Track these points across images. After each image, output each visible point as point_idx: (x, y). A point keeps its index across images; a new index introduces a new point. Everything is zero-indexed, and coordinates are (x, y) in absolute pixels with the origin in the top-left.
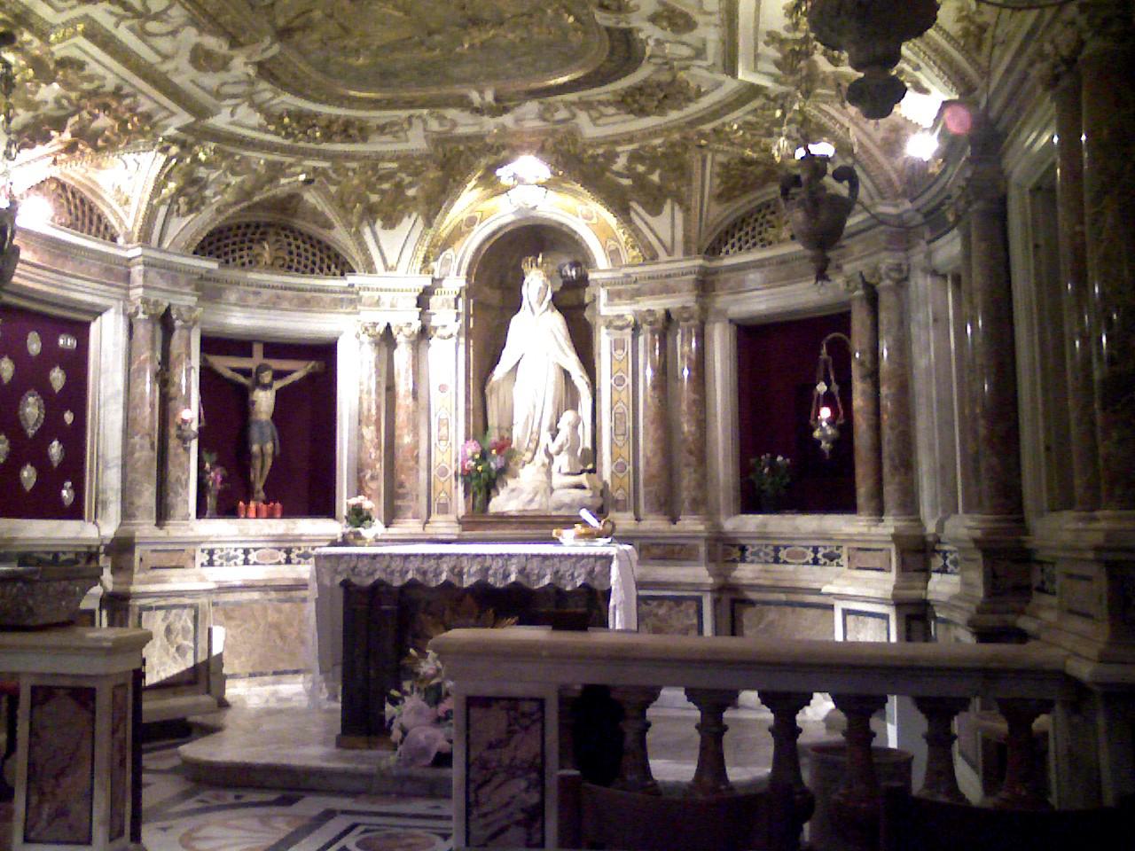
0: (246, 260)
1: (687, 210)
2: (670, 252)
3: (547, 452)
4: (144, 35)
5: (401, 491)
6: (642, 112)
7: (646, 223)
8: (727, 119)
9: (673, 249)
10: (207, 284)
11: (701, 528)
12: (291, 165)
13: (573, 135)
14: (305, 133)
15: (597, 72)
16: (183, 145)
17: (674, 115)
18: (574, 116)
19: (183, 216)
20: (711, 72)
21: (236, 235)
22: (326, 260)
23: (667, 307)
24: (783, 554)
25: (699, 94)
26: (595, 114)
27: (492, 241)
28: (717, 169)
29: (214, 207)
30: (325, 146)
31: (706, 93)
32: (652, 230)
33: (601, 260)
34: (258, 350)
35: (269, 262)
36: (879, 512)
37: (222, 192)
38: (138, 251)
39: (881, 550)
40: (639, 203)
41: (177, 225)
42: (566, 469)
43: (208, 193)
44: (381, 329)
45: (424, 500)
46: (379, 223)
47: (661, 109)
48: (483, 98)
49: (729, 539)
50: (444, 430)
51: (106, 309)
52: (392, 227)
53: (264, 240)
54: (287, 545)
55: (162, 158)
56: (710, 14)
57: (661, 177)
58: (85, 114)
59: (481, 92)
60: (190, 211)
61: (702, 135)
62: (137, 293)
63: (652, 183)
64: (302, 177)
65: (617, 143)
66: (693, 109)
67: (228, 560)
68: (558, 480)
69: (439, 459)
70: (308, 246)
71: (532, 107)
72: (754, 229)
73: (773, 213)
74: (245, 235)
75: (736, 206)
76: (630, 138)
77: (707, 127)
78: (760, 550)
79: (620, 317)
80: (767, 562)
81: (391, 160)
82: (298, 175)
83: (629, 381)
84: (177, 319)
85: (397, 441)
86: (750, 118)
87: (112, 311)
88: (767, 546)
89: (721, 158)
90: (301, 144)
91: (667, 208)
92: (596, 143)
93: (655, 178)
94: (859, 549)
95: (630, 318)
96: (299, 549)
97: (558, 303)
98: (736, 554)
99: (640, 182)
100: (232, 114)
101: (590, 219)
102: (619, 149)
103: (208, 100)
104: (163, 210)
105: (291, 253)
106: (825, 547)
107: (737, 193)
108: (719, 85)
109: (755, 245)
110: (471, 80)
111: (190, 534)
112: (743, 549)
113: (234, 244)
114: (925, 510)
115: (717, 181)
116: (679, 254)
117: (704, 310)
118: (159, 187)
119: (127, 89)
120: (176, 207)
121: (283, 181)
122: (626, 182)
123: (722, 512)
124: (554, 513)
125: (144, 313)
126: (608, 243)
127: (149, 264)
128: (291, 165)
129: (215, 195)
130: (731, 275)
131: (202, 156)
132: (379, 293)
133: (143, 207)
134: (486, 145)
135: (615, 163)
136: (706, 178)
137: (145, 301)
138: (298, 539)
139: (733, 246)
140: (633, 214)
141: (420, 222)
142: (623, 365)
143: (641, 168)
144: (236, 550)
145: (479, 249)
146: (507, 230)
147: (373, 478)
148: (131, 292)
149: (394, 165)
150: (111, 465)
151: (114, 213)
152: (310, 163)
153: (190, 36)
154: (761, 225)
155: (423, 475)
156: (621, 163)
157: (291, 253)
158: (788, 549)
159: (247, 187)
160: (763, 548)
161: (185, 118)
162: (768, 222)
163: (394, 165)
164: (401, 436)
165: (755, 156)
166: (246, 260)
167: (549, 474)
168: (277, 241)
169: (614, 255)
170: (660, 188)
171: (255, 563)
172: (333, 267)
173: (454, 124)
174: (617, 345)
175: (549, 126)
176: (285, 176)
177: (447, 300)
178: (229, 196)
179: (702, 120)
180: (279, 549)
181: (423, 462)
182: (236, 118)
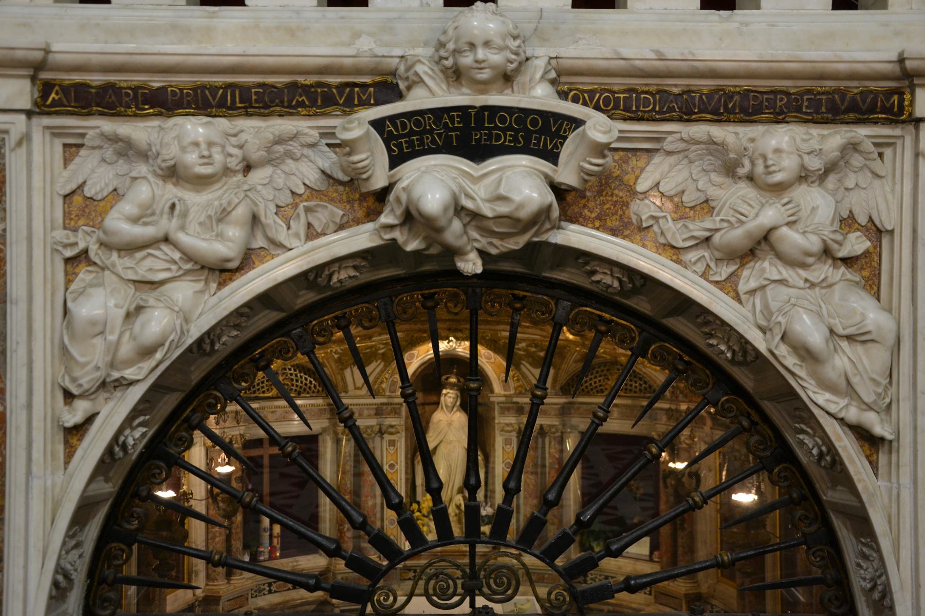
7: (530, 371)
27: (422, 367)
67: (260, 592)
73: (608, 370)
79: (507, 425)
87: (198, 445)
97: (464, 407)
101: (490, 359)
117: (564, 425)
122: (522, 353)
140: (522, 366)
141: (383, 364)
143: (533, 349)
144: (264, 585)
157: (292, 380)
168: (284, 373)
171: (275, 592)
177: (394, 408)
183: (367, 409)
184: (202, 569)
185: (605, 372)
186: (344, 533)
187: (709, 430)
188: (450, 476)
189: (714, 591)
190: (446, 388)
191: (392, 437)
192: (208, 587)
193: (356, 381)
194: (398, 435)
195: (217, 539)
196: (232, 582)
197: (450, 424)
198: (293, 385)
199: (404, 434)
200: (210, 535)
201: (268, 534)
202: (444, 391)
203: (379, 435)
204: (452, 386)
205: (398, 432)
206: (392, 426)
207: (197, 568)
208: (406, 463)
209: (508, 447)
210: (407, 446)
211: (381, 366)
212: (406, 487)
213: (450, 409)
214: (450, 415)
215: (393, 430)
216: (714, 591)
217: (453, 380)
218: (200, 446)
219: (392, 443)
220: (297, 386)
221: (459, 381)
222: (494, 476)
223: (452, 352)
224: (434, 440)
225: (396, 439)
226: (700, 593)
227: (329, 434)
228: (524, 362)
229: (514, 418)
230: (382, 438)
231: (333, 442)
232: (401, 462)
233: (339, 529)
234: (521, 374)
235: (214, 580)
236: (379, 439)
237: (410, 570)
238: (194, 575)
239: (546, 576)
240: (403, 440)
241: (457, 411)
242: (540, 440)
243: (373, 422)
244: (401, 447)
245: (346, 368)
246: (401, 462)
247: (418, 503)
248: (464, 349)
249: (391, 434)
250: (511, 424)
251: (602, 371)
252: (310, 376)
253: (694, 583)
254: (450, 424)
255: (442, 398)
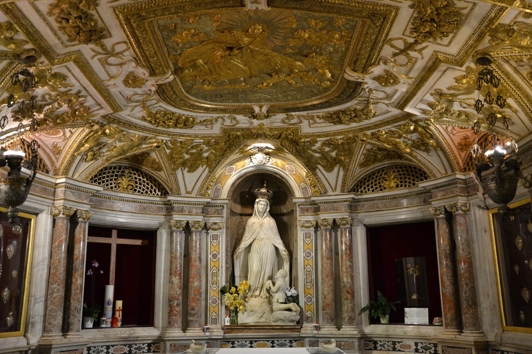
0: (113, 185)
1: (346, 171)
2: (334, 190)
3: (268, 291)
4: (104, 63)
5: (193, 312)
6: (340, 122)
7: (324, 175)
8: (381, 129)
9: (335, 190)
10: (95, 198)
11: (356, 332)
12: (151, 138)
13: (296, 131)
14: (164, 122)
15: (326, 102)
16: (102, 126)
17: (354, 125)
18: (301, 122)
19: (88, 162)
20: (388, 107)
21: (109, 173)
22: (154, 187)
23: (334, 218)
24: (398, 346)
25: (374, 115)
26: (311, 121)
27: (240, 180)
28: (365, 152)
29: (104, 158)
30: (171, 130)
31: (378, 115)
32: (326, 179)
33: (298, 193)
34: (114, 233)
35: (125, 187)
36: (460, 327)
37: (112, 150)
38: (63, 180)
39: (465, 348)
40: (321, 165)
41: (84, 166)
42: (282, 300)
43: (104, 150)
44: (184, 224)
45: (203, 316)
46: (187, 169)
47: (352, 120)
48: (261, 111)
49: (368, 337)
50: (215, 278)
51: (42, 211)
52: (194, 171)
53: (123, 175)
54: (130, 343)
55: (87, 131)
56: (411, 78)
57: (337, 154)
58: (56, 105)
59: (261, 107)
60: (92, 160)
61: (365, 135)
62: (59, 203)
63: (331, 157)
64: (155, 144)
65: (319, 136)
66: (365, 123)
68: (276, 306)
69: (212, 294)
70: (145, 179)
71: (282, 116)
72: (376, 181)
73: (386, 174)
74: (113, 172)
75: (369, 168)
76: (327, 135)
77: (369, 133)
78: (385, 344)
80: (389, 350)
81: (201, 138)
82: (153, 143)
83: (313, 254)
84: (80, 217)
85: (190, 285)
86: (392, 129)
87: (45, 212)
88: (388, 342)
89: (369, 147)
90: (159, 128)
91: (336, 169)
92: (306, 136)
93: (334, 154)
94: (449, 347)
95: (314, 223)
96: (136, 345)
97: (273, 214)
98: (372, 345)
99: (324, 156)
100: (131, 111)
102: (318, 139)
103: (121, 101)
104: (79, 158)
105: (136, 183)
106: (422, 343)
107: (370, 163)
108: (388, 112)
109: (376, 188)
110: (258, 101)
111: (82, 340)
112: (375, 343)
113: (108, 177)
114: (486, 327)
115: (363, 157)
116: (338, 191)
118: (81, 145)
119: (84, 93)
120: (86, 157)
121: (144, 146)
122: (318, 155)
123: (363, 323)
124: (274, 324)
125: (63, 214)
126: (301, 185)
127: (68, 187)
128: (151, 138)
129: (107, 151)
130: (366, 203)
131: (107, 131)
132: (183, 205)
133: (68, 157)
134: (252, 133)
135: (315, 146)
136: (359, 156)
137: (65, 208)
138: (137, 339)
139: (365, 188)
140: (318, 171)
141: (207, 169)
142: (310, 246)
143: (327, 149)
144: (102, 347)
145: (233, 184)
146: (249, 175)
147: (177, 305)
148: (56, 202)
149: (202, 141)
150: (38, 301)
151: (50, 158)
152: (160, 138)
153: (131, 67)
154: (380, 179)
155: (203, 303)
156: (318, 145)
157: (136, 183)
158: (400, 344)
159: (125, 148)
160: (386, 343)
161: (107, 110)
162: (383, 178)
163: (202, 141)
164: (193, 282)
165: (389, 146)
166: (113, 185)
167: (270, 303)
168: (130, 176)
169: (304, 190)
170: (335, 159)
172: (157, 190)
173: (238, 122)
174: (307, 236)
175: (286, 126)
176: (145, 144)
177: (217, 210)
178: (114, 153)
179: (368, 128)
180: (125, 345)
181: (203, 296)
182: (132, 113)
183: (196, 208)
184: (39, 321)
185: (383, 175)
186: (174, 307)
187: (482, 195)
188: (262, 267)
189: (501, 340)
190: (258, 198)
191: (215, 233)
192: (43, 338)
193: (187, 185)
194: (220, 230)
195: (55, 295)
196: (68, 337)
197: (261, 225)
198: (137, 187)
199: (224, 230)
200: (50, 291)
201: (111, 306)
202: (257, 200)
203: (205, 231)
204: (263, 195)
205: (220, 228)
206: (215, 223)
207: (33, 320)
208: (227, 255)
209: (308, 239)
210: (227, 241)
211: (206, 172)
212: (226, 274)
213: (262, 214)
214: (261, 219)
215: (216, 227)
216: (501, 340)
217: (263, 190)
218: (47, 213)
219: (215, 237)
220: (140, 188)
221: (268, 191)
222: (297, 264)
223: (263, 167)
224: (249, 239)
225: (219, 234)
226: (487, 342)
227: (165, 228)
228: (319, 166)
229: (312, 217)
230: (207, 233)
231: (167, 235)
232: (222, 253)
233: (170, 304)
234: (317, 179)
235: (50, 331)
236: (205, 234)
237: (229, 342)
238: (30, 326)
239: (343, 343)
240: (224, 235)
241: (267, 216)
242: (333, 234)
243: (200, 218)
244: (222, 241)
245: (177, 169)
246: (222, 253)
247: (236, 287)
248: (272, 164)
249: (215, 229)
250: (310, 221)
251: (381, 175)
252: (151, 182)
253: (480, 333)
254: (261, 225)
255: (256, 206)
